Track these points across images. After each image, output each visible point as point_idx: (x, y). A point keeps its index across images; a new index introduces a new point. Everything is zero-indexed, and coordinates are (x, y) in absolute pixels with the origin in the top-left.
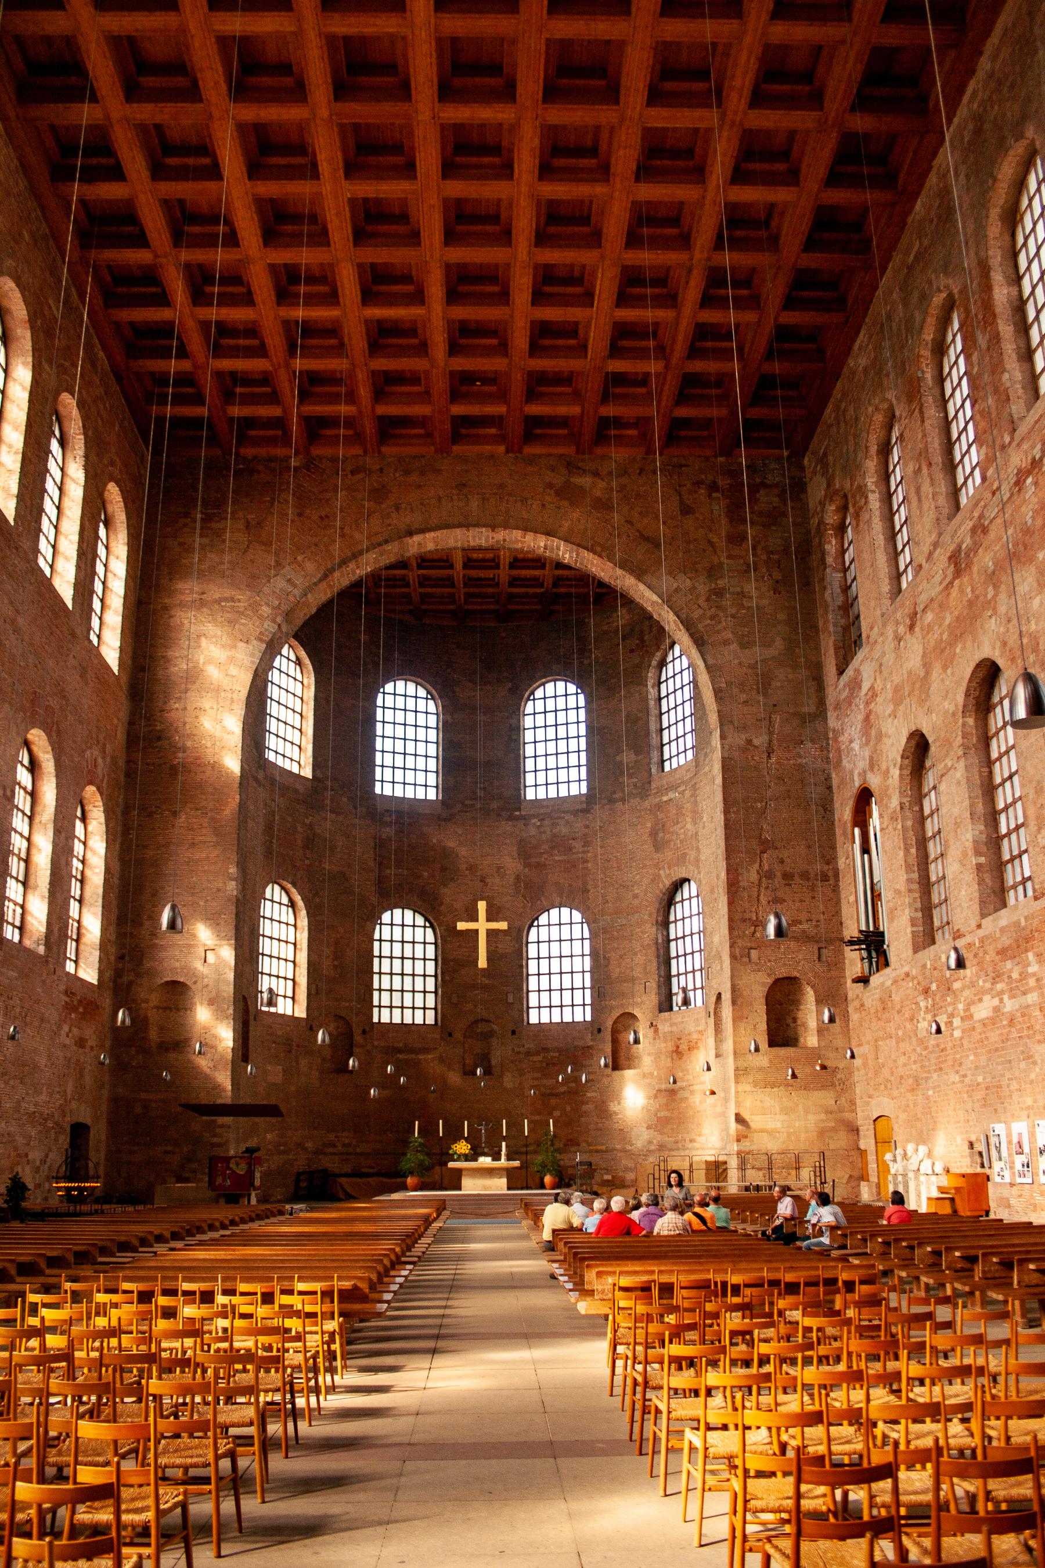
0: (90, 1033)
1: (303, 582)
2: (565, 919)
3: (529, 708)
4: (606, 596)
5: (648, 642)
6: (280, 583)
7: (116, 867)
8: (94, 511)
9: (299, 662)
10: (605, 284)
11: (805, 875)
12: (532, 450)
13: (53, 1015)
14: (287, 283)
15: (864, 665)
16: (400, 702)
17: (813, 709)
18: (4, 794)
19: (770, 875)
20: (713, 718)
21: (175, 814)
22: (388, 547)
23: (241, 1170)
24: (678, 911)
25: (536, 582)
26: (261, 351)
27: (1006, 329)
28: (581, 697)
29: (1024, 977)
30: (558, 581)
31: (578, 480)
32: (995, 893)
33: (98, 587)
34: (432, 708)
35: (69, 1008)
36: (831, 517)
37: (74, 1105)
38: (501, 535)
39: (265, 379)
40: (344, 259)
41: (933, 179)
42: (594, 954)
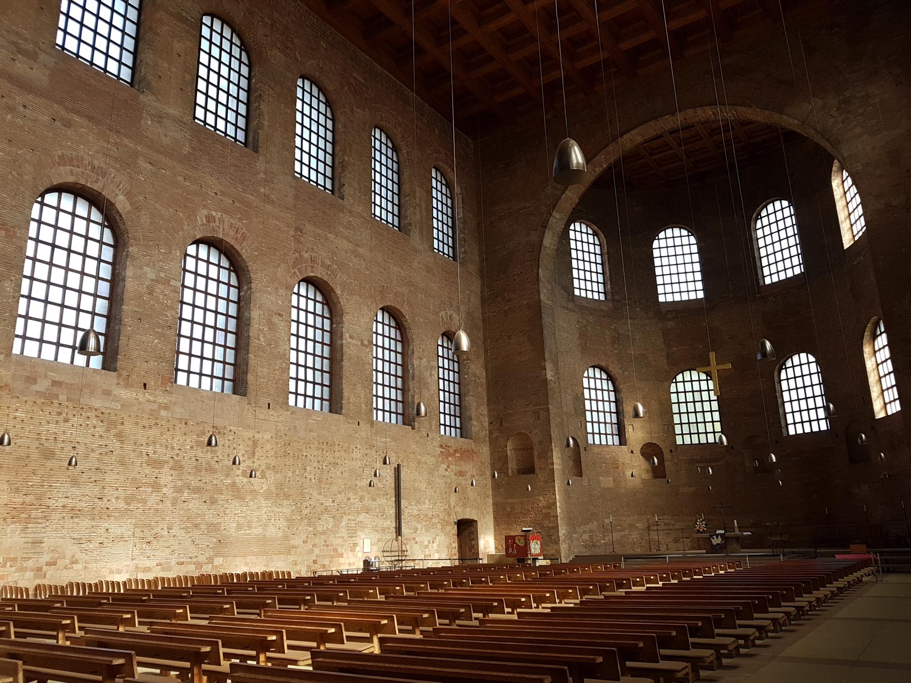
2: (804, 360)
9: (595, 234)
16: (670, 242)
18: (362, 344)
21: (510, 337)
22: (610, 148)
23: (521, 543)
34: (693, 240)
37: (459, 509)
42: (826, 383)
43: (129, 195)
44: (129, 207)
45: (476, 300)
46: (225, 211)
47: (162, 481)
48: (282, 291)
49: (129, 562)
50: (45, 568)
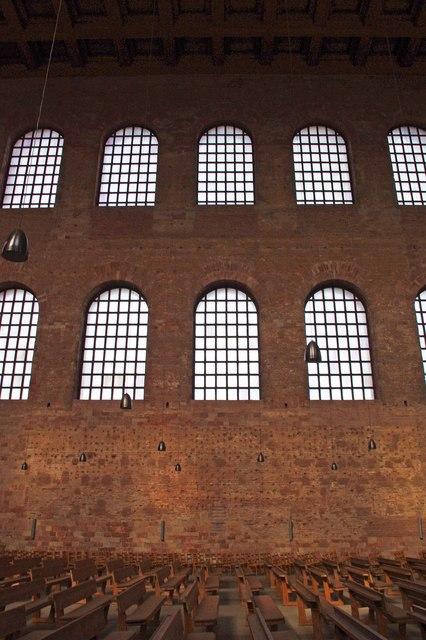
43: (256, 275)
44: (256, 282)
47: (310, 477)
48: (403, 303)
50: (227, 541)
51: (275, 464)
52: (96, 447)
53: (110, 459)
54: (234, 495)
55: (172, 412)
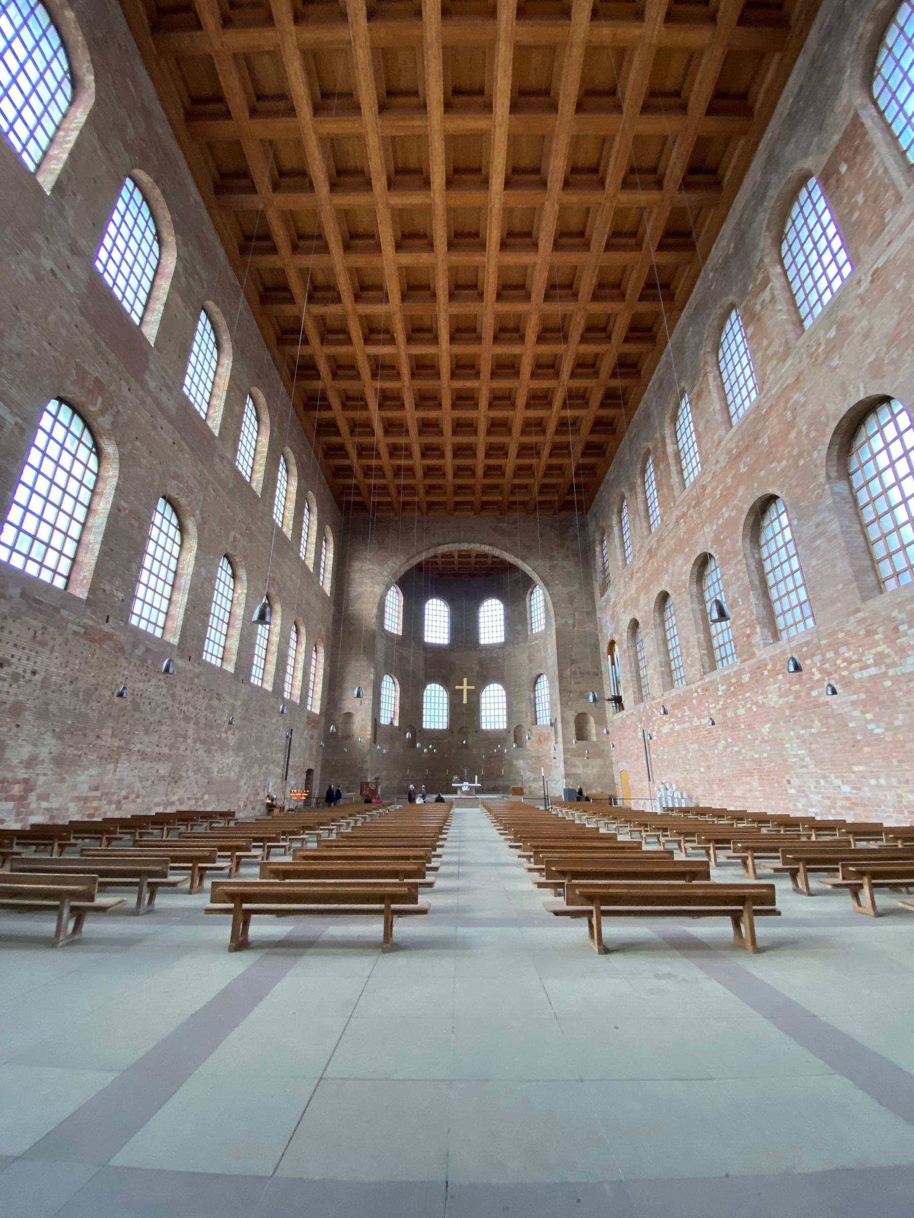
0: (316, 733)
1: (398, 564)
3: (482, 609)
4: (512, 568)
5: (527, 584)
6: (390, 563)
7: (328, 669)
8: (321, 535)
10: (513, 451)
11: (589, 673)
12: (484, 513)
13: (301, 726)
14: (394, 450)
15: (611, 593)
17: (590, 609)
19: (575, 673)
20: (552, 613)
23: (373, 787)
24: (538, 687)
25: (485, 563)
26: (384, 476)
27: (672, 461)
28: (502, 606)
29: (683, 716)
30: (493, 563)
31: (502, 525)
32: (669, 681)
33: (322, 564)
34: (446, 609)
35: (308, 723)
36: (598, 537)
38: (472, 546)
39: (385, 487)
40: (415, 441)
41: (642, 404)
45: (331, 619)
46: (241, 534)
49: (164, 798)
51: (172, 718)
52: (14, 651)
53: (28, 675)
54: (138, 746)
55: (110, 631)
